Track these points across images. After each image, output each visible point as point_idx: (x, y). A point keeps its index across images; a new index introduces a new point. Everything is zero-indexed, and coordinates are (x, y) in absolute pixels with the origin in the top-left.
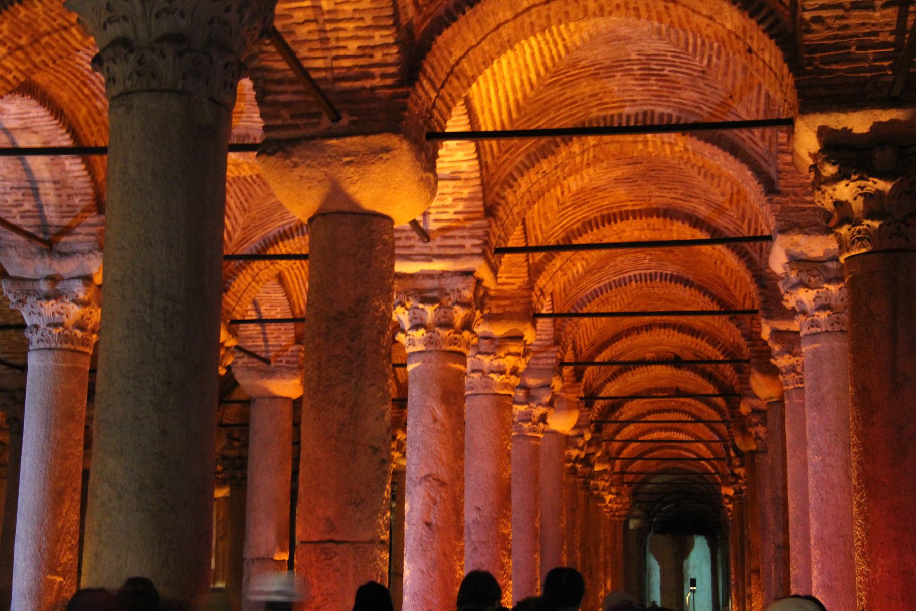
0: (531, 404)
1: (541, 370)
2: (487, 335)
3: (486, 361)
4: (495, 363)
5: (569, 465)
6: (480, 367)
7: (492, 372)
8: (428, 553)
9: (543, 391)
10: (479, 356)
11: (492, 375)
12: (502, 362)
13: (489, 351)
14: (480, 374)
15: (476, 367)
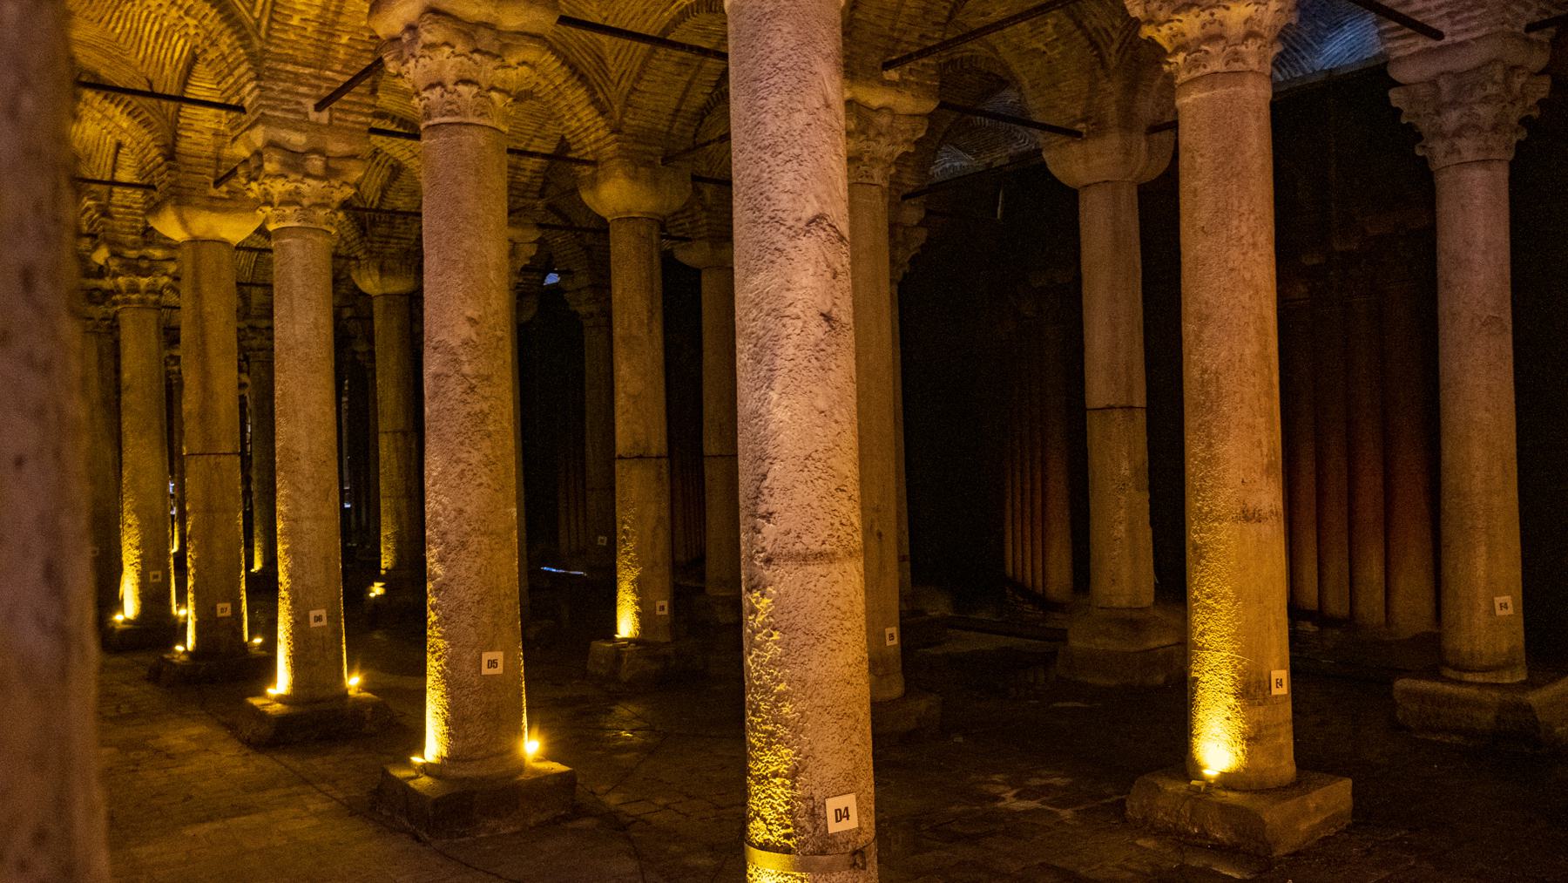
0: (333, 182)
1: (352, 130)
2: (490, 21)
3: (490, 65)
4: (500, 73)
5: (153, 297)
6: (473, 76)
7: (493, 88)
8: (832, 375)
9: (352, 164)
10: (477, 57)
11: (494, 94)
12: (512, 73)
13: (495, 51)
14: (475, 90)
15: (467, 76)
